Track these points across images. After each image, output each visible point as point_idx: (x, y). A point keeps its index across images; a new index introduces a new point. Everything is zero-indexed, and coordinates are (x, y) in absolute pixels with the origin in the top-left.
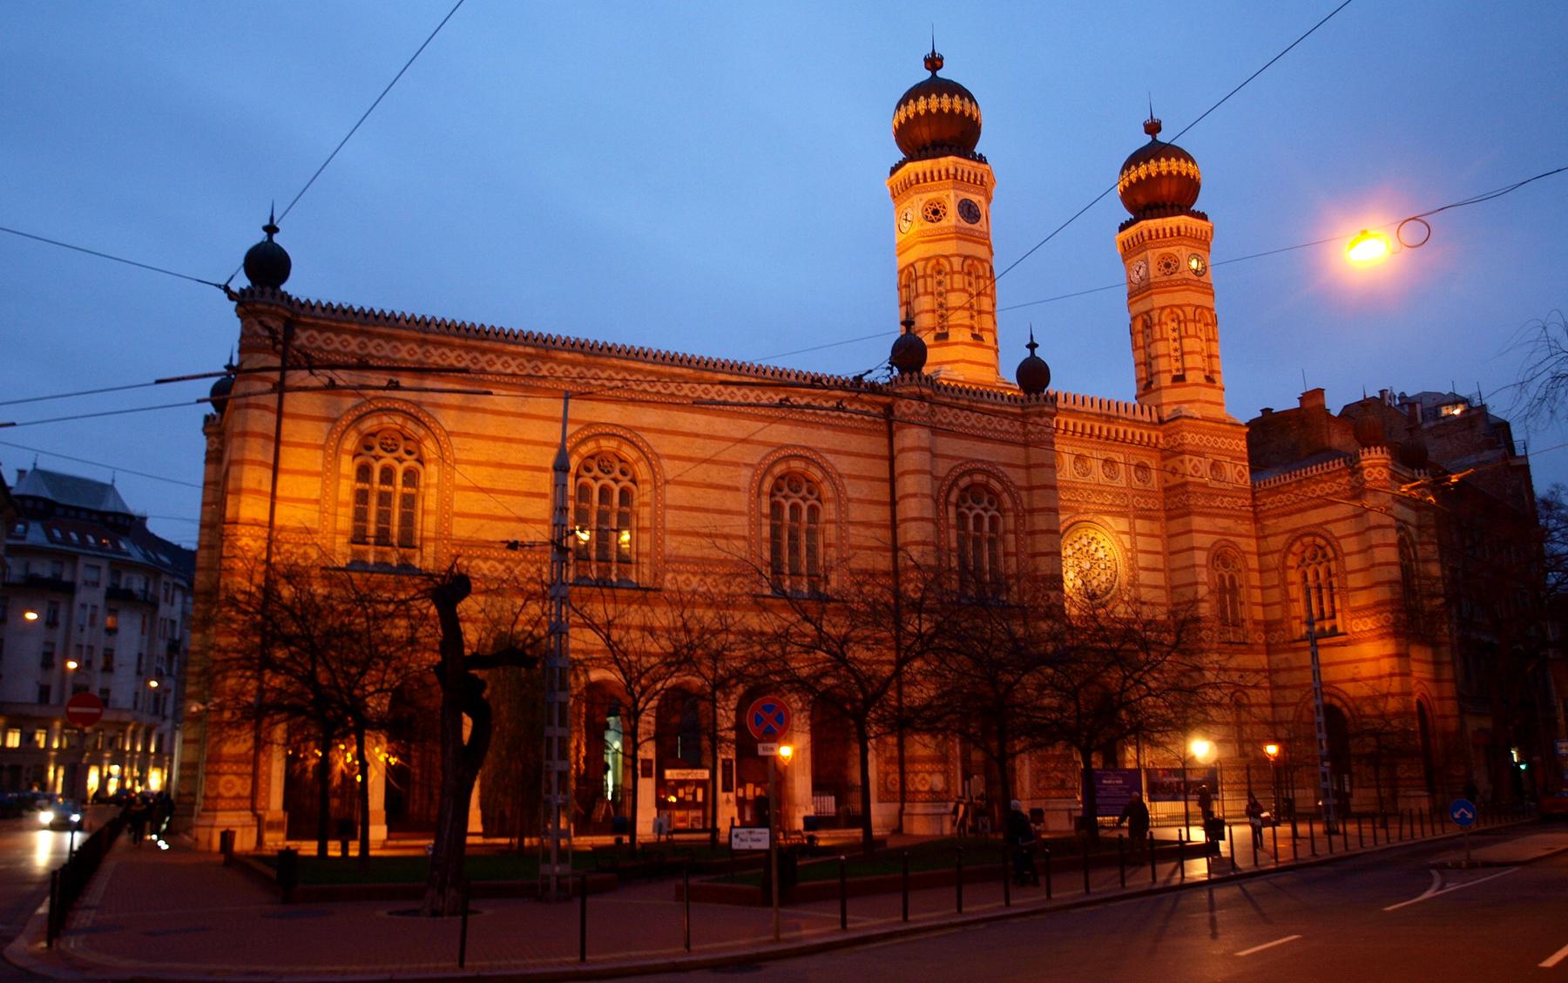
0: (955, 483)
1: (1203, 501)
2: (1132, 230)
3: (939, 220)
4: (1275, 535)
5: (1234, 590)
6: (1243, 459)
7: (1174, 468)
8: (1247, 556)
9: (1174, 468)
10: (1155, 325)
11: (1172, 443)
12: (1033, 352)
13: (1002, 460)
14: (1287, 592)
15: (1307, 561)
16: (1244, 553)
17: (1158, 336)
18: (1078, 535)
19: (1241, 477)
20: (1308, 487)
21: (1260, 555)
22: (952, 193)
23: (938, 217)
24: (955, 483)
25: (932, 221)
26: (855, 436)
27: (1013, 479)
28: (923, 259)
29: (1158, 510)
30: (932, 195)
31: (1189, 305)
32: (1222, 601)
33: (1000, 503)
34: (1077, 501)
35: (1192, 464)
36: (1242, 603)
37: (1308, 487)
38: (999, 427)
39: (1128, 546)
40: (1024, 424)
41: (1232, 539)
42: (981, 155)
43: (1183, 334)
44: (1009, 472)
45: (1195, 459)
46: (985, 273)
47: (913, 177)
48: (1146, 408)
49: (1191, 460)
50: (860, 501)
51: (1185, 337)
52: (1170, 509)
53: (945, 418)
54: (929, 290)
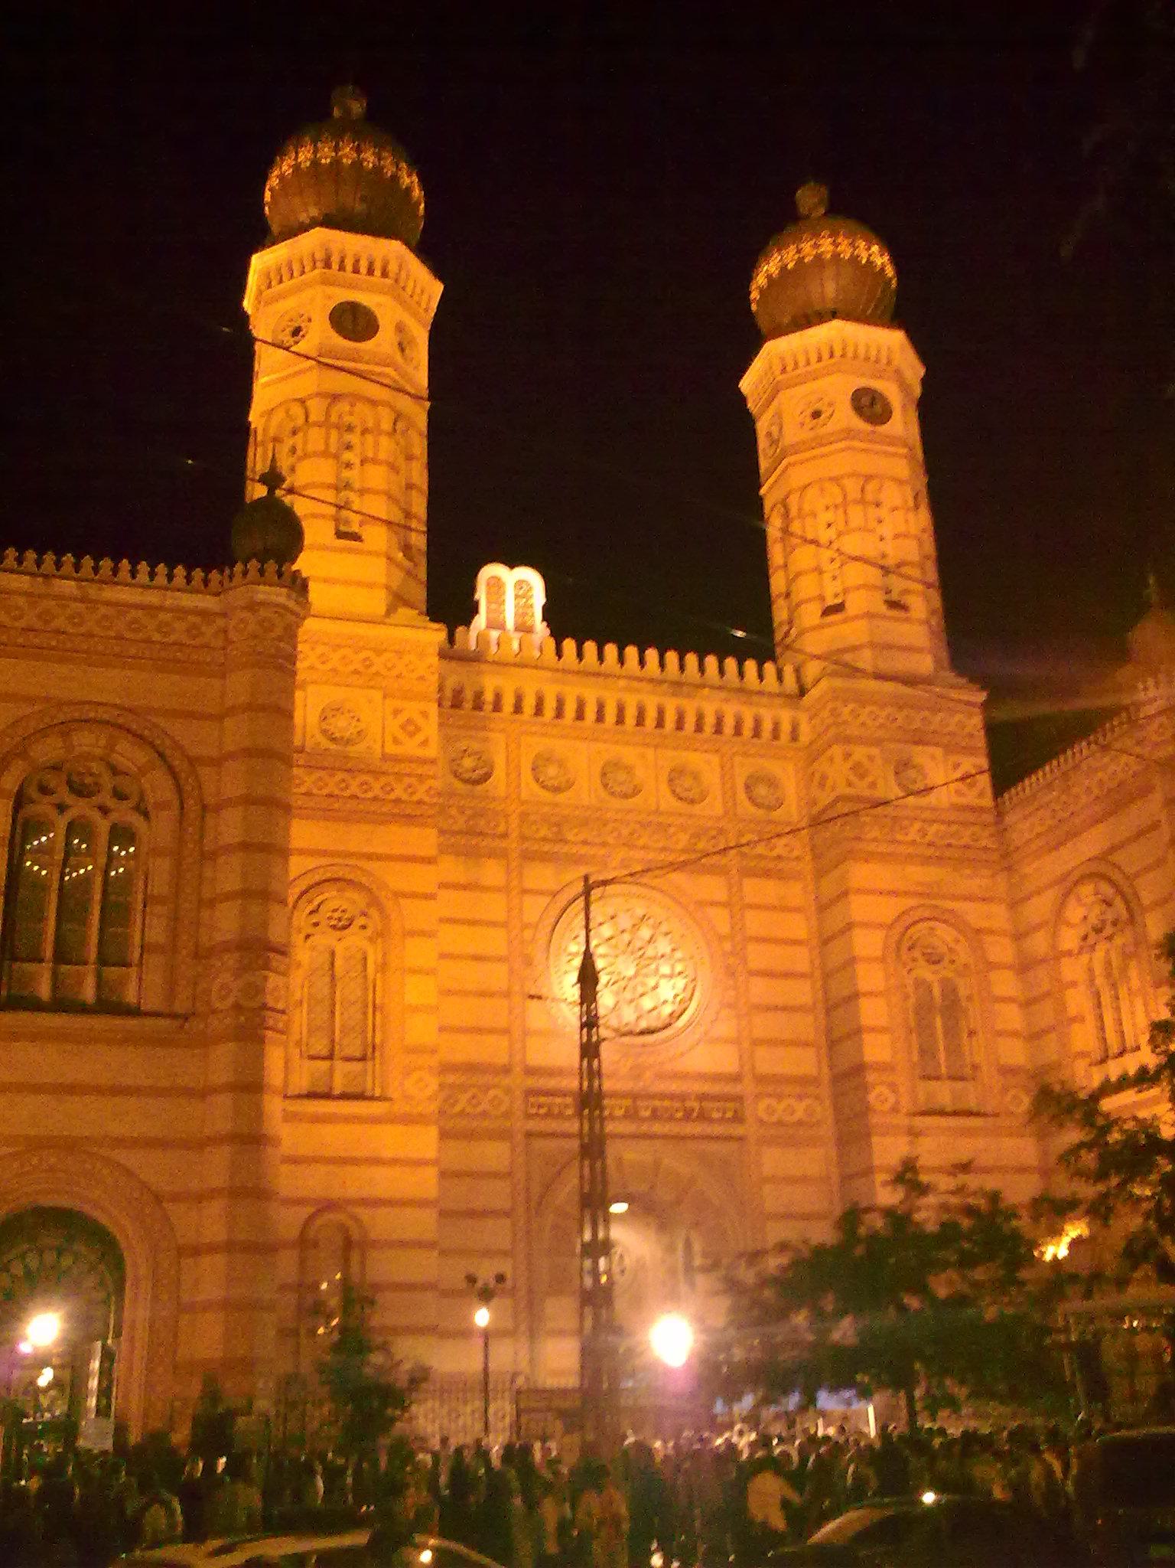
4: (1038, 892)
5: (952, 1006)
14: (1062, 1007)
15: (1091, 940)
16: (979, 931)
18: (611, 911)
22: (318, 292)
29: (798, 858)
30: (289, 304)
32: (922, 1025)
36: (972, 1033)
38: (157, 637)
39: (724, 928)
41: (950, 905)
44: (178, 729)
46: (378, 424)
49: (848, 756)
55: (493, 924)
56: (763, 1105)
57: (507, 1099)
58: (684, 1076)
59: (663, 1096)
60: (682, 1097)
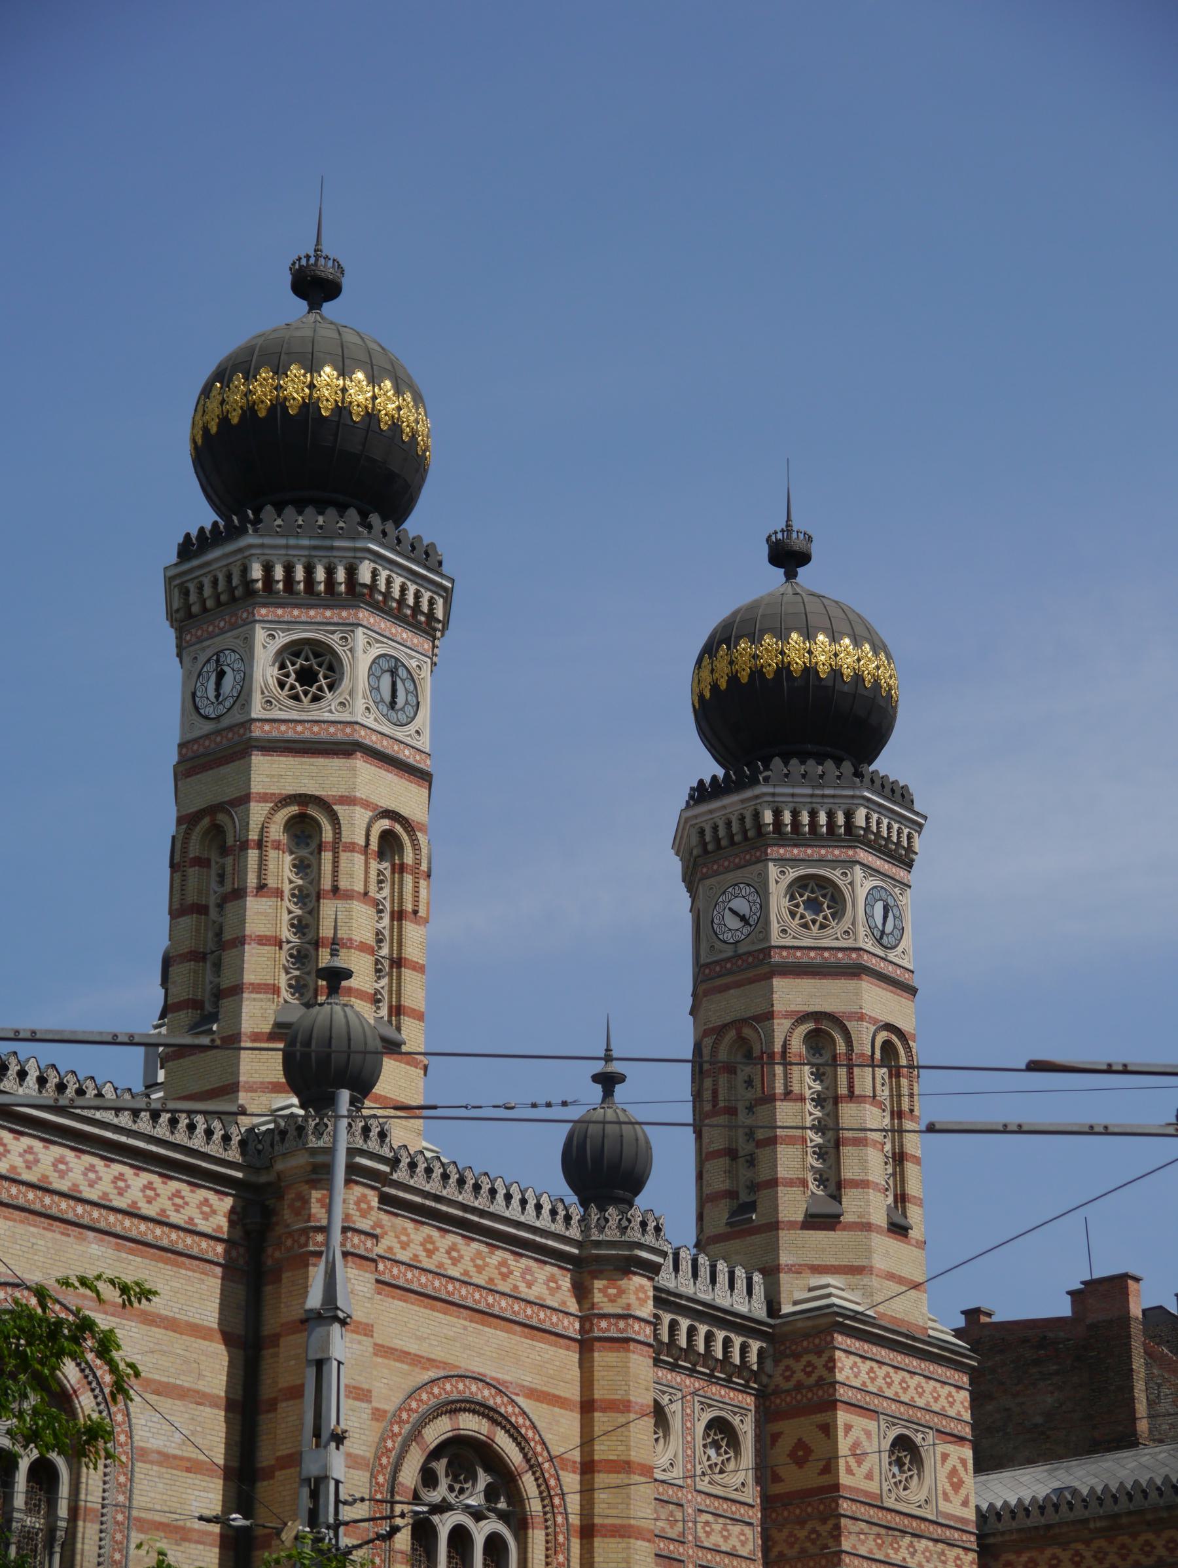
0: (416, 1434)
1: (871, 1543)
2: (731, 802)
3: (316, 699)
6: (961, 1439)
7: (801, 1444)
9: (801, 1444)
12: (608, 1093)
13: (528, 1379)
19: (957, 1486)
20: (1134, 1536)
23: (314, 689)
24: (416, 1434)
25: (296, 698)
26: (168, 1270)
27: (547, 1437)
28: (264, 798)
31: (861, 1017)
33: (516, 1497)
37: (1134, 1536)
38: (522, 1287)
40: (581, 1291)
42: (432, 545)
43: (843, 1090)
44: (538, 1412)
46: (418, 863)
47: (257, 572)
48: (740, 1272)
49: (848, 1428)
50: (166, 1459)
53: (404, 1246)
54: (271, 882)
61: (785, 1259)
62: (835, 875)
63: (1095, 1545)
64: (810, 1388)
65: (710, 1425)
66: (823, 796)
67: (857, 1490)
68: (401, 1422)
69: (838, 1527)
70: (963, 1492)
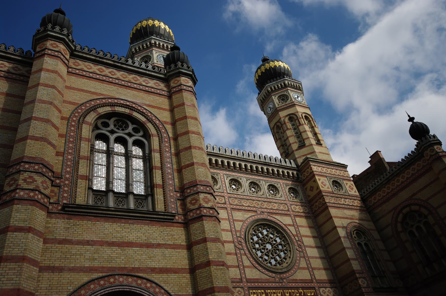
0: (94, 109)
8: (371, 232)
10: (283, 125)
11: (306, 175)
13: (148, 103)
17: (285, 129)
19: (352, 189)
21: (380, 231)
24: (94, 109)
34: (254, 207)
35: (321, 181)
38: (144, 84)
40: (168, 86)
45: (322, 179)
49: (319, 180)
51: (299, 126)
52: (316, 211)
55: (227, 231)
56: (321, 290)
57: (242, 291)
58: (295, 281)
59: (291, 288)
60: (297, 288)
61: (297, 156)
62: (285, 93)
63: (386, 187)
64: (309, 175)
65: (290, 189)
66: (278, 82)
67: (326, 191)
68: (86, 106)
69: (324, 198)
70: (354, 190)
